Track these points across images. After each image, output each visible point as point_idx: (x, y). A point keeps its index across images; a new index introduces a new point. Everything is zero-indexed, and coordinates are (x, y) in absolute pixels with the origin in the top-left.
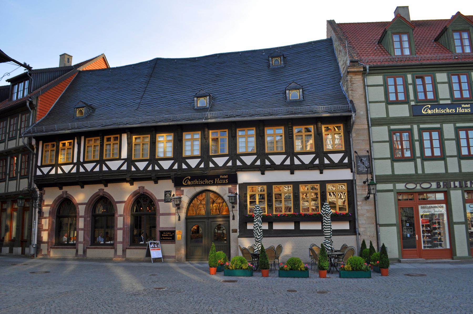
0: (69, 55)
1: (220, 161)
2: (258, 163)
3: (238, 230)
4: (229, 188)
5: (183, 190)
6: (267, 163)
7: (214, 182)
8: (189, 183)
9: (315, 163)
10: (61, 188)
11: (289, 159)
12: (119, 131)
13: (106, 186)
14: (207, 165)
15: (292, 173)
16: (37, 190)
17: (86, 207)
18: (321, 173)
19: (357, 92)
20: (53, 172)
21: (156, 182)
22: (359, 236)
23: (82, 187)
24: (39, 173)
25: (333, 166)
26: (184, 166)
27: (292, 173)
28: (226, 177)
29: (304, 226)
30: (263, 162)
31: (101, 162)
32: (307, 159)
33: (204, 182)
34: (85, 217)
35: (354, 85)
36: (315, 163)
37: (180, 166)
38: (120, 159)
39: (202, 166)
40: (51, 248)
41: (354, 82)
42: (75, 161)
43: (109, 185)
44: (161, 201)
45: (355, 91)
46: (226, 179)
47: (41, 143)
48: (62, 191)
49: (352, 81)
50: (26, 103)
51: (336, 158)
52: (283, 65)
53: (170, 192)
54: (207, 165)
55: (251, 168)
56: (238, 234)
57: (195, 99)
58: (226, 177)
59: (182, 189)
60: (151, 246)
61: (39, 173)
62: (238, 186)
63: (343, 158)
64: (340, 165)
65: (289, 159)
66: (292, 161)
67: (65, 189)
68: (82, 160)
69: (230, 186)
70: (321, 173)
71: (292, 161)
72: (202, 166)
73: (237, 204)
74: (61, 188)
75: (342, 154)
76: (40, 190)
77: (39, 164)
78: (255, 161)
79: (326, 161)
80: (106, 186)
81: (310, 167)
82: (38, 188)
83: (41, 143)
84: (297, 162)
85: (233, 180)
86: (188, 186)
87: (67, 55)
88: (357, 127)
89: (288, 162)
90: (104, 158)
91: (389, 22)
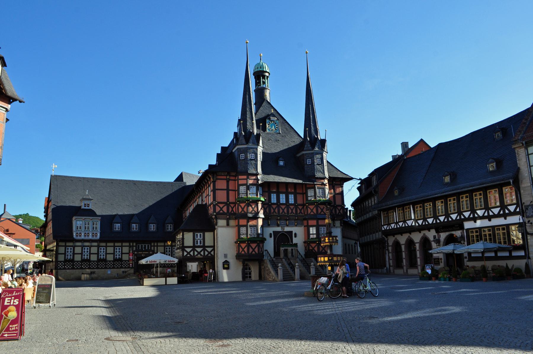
0: (406, 142)
1: (454, 216)
2: (471, 216)
3: (468, 257)
4: (461, 232)
5: (440, 235)
6: (476, 216)
7: (453, 228)
8: (442, 230)
9: (501, 213)
10: (394, 236)
11: (487, 212)
12: (409, 204)
13: (411, 234)
14: (448, 219)
15: (490, 220)
16: (385, 238)
17: (405, 246)
18: (505, 219)
19: (522, 161)
20: (388, 228)
21: (429, 231)
22: (529, 260)
23: (402, 235)
24: (383, 229)
25: (511, 214)
26: (438, 221)
27: (490, 220)
28: (458, 226)
29: (514, 254)
30: (474, 215)
31: (405, 221)
32: (496, 211)
33: (449, 230)
34: (405, 252)
35: (520, 156)
36: (501, 213)
37: (436, 221)
38: (411, 219)
39: (446, 220)
40: (394, 269)
41: (520, 154)
42: (395, 222)
43: (412, 233)
44: (432, 241)
45: (521, 160)
46: (457, 227)
47: (382, 212)
48: (394, 237)
49: (518, 153)
50: (372, 191)
51: (512, 208)
52: (502, 138)
53: (435, 236)
54: (448, 219)
55: (468, 219)
56: (467, 259)
57: (444, 178)
58: (458, 226)
59: (440, 234)
60: (427, 267)
61: (383, 229)
62: (465, 230)
63: (516, 209)
64: (515, 213)
65: (487, 212)
66: (488, 213)
67: (396, 236)
68: (398, 221)
69: (461, 231)
70: (505, 219)
71: (488, 213)
72: (446, 220)
73: (465, 241)
74: (394, 236)
75: (515, 206)
76: (386, 238)
77: (383, 224)
78: (470, 215)
79: (507, 211)
80: (411, 234)
81: (498, 216)
82: (385, 236)
83: (382, 212)
84: (491, 214)
85: (461, 227)
86: (442, 232)
87: (404, 142)
88: (524, 186)
89: (486, 214)
90: (406, 219)
91: (528, 110)
